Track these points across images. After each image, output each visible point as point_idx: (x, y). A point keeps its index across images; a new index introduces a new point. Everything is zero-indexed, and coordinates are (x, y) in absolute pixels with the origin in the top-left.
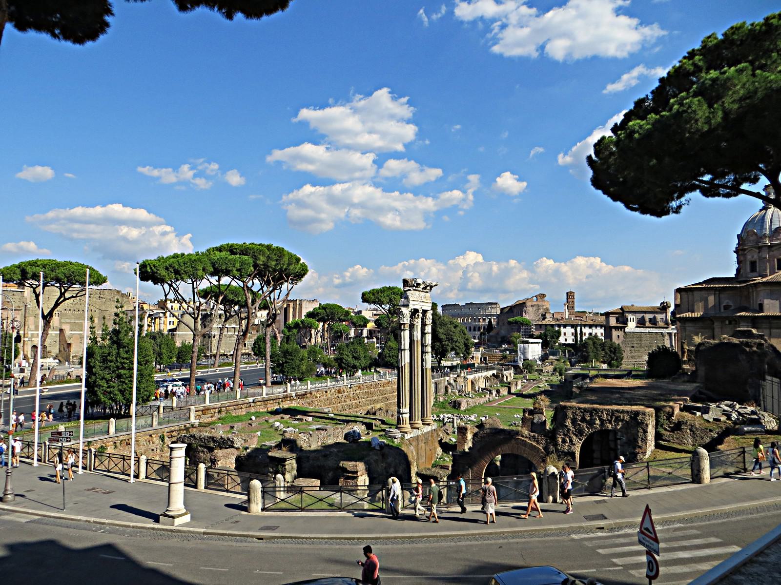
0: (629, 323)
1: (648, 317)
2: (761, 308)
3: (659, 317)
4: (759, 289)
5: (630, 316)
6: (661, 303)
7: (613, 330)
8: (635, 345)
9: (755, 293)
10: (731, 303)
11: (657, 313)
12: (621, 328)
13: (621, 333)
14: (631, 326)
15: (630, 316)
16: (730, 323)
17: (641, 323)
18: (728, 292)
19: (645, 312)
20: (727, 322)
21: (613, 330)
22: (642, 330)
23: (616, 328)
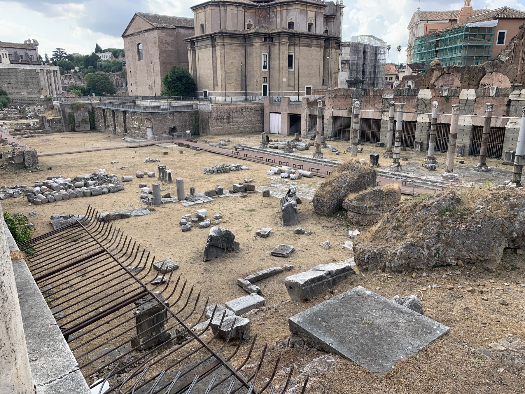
4: (290, 8)
8: (12, 82)
9: (284, 12)
10: (252, 23)
16: (265, 41)
18: (250, 11)
20: (263, 39)
22: (13, 66)
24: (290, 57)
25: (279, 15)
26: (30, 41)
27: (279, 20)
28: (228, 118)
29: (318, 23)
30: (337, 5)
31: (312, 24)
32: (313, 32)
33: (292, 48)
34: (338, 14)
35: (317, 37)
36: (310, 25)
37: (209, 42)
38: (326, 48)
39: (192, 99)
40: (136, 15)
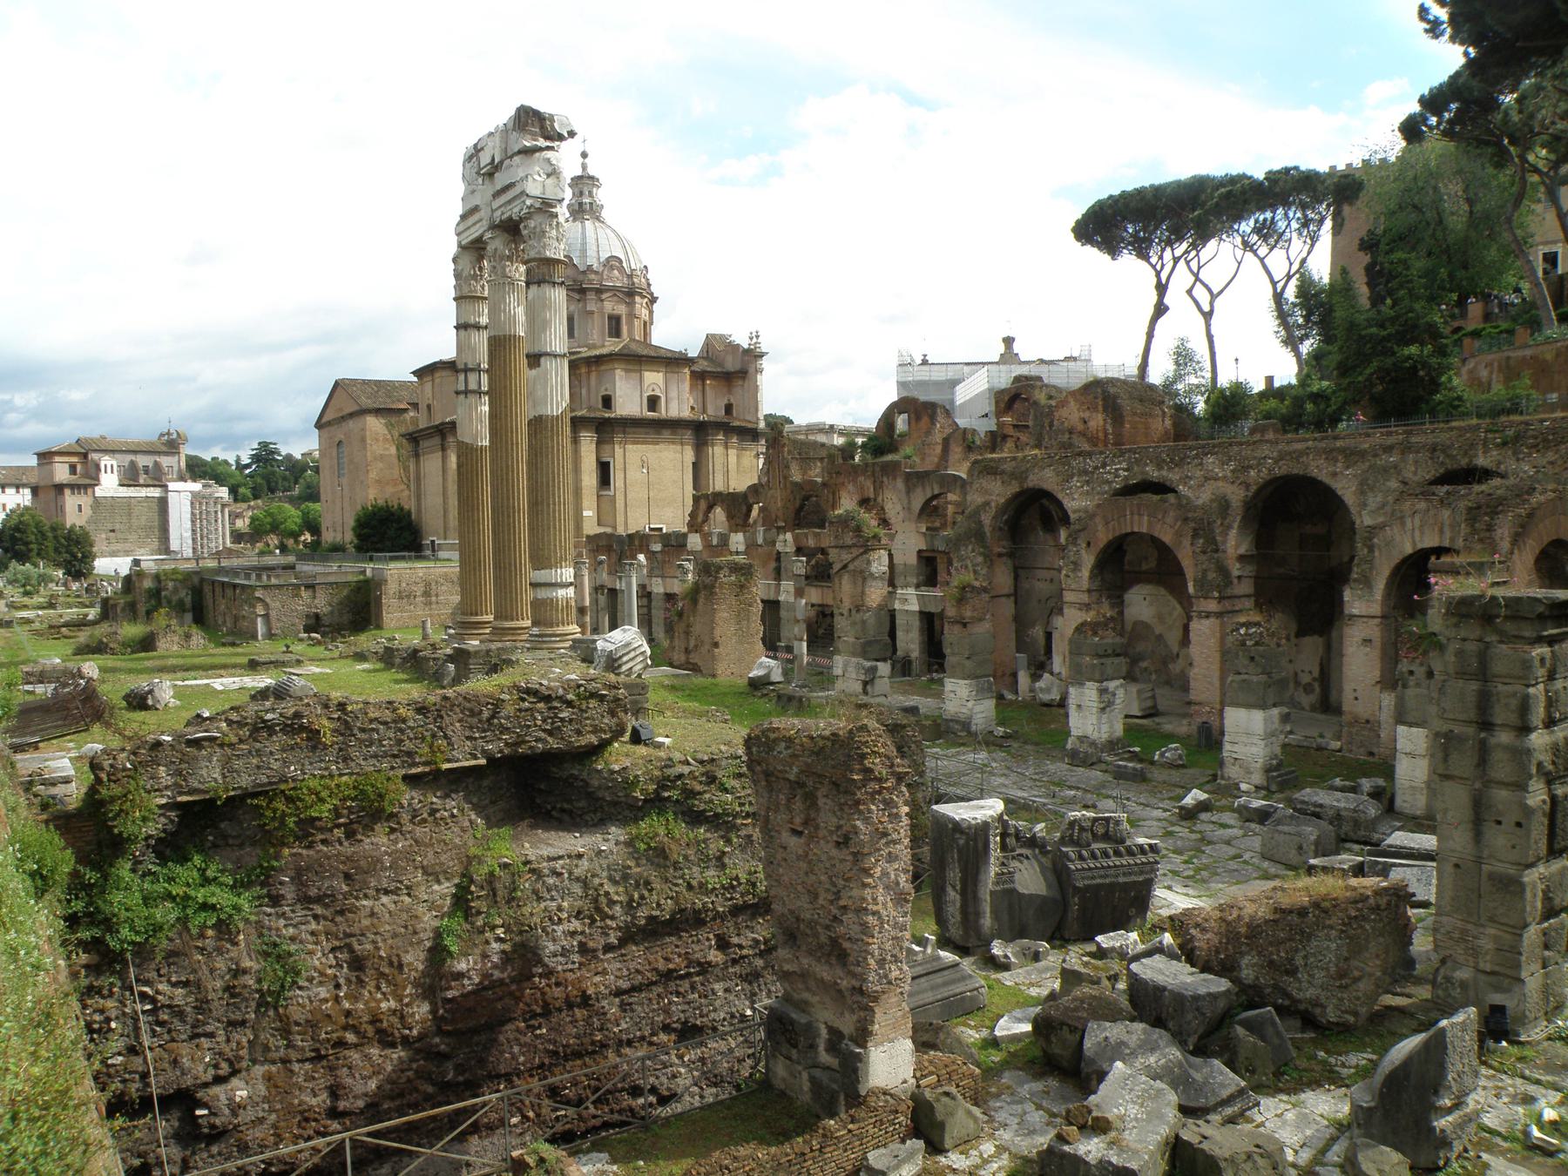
0: (104, 477)
1: (143, 461)
2: (607, 402)
3: (165, 461)
5: (106, 461)
6: (162, 435)
7: (67, 492)
8: (117, 527)
9: (593, 375)
11: (159, 453)
12: (86, 487)
13: (84, 500)
14: (109, 484)
15: (106, 461)
17: (130, 477)
19: (135, 452)
21: (67, 492)
23: (74, 487)
24: (604, 470)
25: (584, 383)
26: (168, 433)
27: (584, 391)
28: (426, 594)
29: (673, 394)
30: (747, 352)
31: (658, 398)
32: (663, 413)
33: (607, 447)
34: (751, 370)
35: (673, 426)
36: (653, 402)
37: (437, 440)
38: (700, 446)
39: (410, 558)
40: (337, 384)
